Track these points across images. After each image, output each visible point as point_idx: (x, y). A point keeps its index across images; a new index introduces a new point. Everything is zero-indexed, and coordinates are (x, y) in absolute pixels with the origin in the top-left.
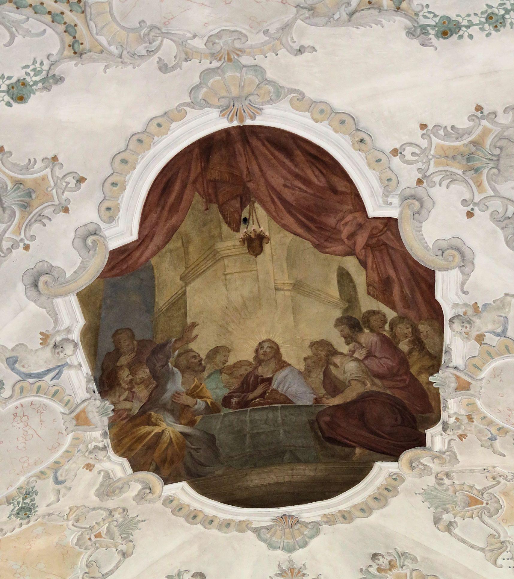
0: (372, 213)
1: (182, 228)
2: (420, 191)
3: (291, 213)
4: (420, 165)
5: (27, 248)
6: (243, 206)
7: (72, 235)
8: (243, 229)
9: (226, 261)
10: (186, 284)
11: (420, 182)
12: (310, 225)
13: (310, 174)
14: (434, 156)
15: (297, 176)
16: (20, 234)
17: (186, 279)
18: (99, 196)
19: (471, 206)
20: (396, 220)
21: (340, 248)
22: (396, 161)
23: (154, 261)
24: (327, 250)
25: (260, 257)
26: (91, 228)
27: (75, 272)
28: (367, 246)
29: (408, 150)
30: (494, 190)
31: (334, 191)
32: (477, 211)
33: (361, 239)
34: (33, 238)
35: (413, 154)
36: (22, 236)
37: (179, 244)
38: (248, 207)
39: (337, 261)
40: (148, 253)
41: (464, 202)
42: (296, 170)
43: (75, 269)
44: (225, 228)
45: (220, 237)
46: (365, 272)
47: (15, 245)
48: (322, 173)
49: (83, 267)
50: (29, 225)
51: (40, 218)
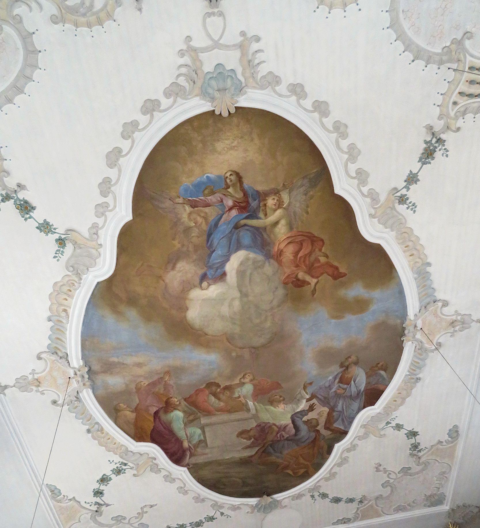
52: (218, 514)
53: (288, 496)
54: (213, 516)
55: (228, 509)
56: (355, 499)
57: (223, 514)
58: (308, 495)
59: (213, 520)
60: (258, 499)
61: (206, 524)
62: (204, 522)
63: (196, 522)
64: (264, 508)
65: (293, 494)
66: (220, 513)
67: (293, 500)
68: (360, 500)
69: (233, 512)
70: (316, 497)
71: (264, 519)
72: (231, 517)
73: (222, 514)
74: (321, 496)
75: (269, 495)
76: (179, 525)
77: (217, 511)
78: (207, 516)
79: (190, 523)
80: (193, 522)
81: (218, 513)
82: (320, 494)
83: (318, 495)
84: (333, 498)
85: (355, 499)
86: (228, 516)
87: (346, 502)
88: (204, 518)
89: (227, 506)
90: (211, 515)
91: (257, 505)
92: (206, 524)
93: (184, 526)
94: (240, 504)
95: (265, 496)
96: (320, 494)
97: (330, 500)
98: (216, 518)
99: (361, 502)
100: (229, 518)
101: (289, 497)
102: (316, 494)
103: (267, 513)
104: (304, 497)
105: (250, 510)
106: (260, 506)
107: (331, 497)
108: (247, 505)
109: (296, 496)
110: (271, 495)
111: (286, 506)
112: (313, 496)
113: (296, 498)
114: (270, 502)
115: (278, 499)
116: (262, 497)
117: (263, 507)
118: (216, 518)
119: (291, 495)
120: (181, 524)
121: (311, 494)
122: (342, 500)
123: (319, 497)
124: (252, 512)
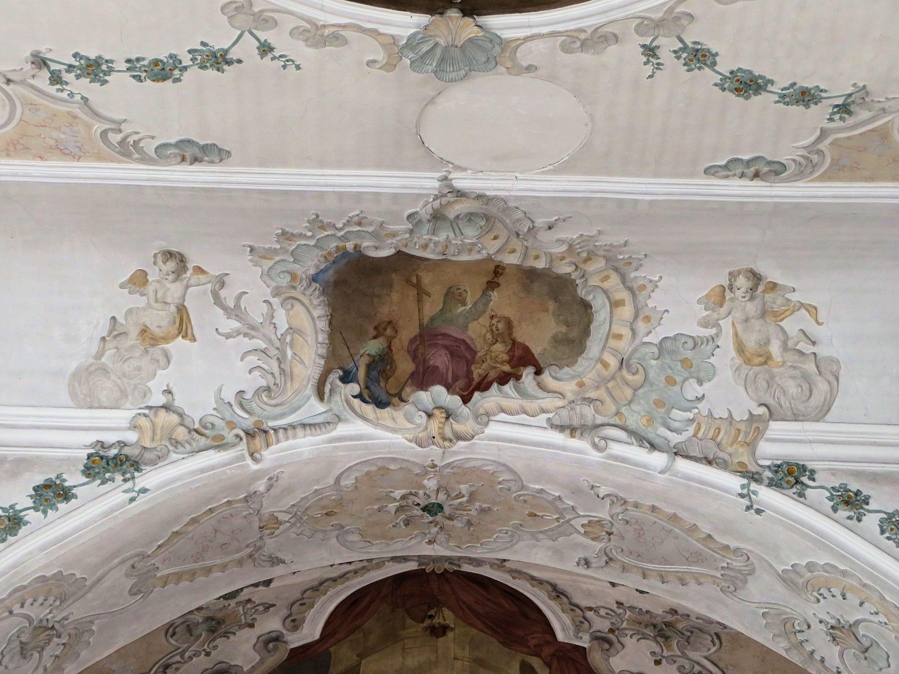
0: (561, 636)
1: (366, 626)
2: (611, 636)
3: (479, 619)
4: (614, 621)
5: (208, 654)
6: (430, 608)
7: (254, 641)
8: (427, 622)
9: (406, 641)
10: (362, 659)
11: (611, 631)
12: (499, 630)
13: (503, 602)
14: (627, 620)
15: (488, 600)
16: (203, 646)
17: (361, 656)
18: (285, 612)
19: (660, 657)
20: (585, 648)
21: (525, 650)
22: (590, 614)
23: (332, 649)
24: (512, 648)
25: (441, 639)
26: (273, 635)
27: (253, 667)
28: (553, 655)
29: (603, 612)
30: (683, 653)
31: (526, 616)
32: (664, 661)
33: (547, 651)
34: (215, 647)
35: (607, 614)
36: (206, 647)
37: (361, 635)
38: (435, 609)
39: (520, 657)
40: (328, 645)
41: (653, 653)
42: (490, 597)
43: (253, 664)
44: (409, 621)
45: (404, 627)
46: (548, 670)
47: (196, 654)
48: (515, 604)
49: (262, 661)
50: (214, 640)
51: (226, 635)
52: (247, 49)
53: (545, 30)
54: (226, 51)
55: (291, 33)
56: (823, 95)
57: (271, 49)
58: (632, 47)
59: (226, 67)
60: (421, 19)
61: (193, 75)
62: (185, 68)
63: (156, 62)
64: (442, 60)
65: (572, 26)
66: (257, 44)
67: (566, 48)
68: (840, 101)
69: (310, 51)
70: (665, 55)
71: (432, 101)
72: (298, 67)
73: (265, 49)
74: (684, 55)
75: (470, 10)
76: (81, 58)
77: (247, 34)
78: (203, 44)
79: (129, 61)
80: (144, 59)
81: (249, 45)
82: (685, 48)
83: (675, 52)
84: (732, 72)
85: (823, 95)
86: (287, 61)
87: (783, 98)
88: (190, 52)
89: (289, 23)
90: (219, 44)
91: (412, 43)
92: (193, 75)
93: (104, 67)
94: (344, 26)
95: (454, 14)
96: (685, 48)
97: (717, 78)
98: (239, 61)
99: (844, 109)
100: (291, 68)
101: (553, 34)
102: (667, 45)
103: (451, 81)
104: (613, 49)
105: (380, 56)
106: (425, 48)
107: (724, 66)
108: (374, 33)
109: (583, 36)
110: (479, 15)
111: (530, 69)
112: (650, 51)
113: (578, 44)
114: (471, 40)
115: (507, 35)
116: (441, 14)
117: (438, 52)
118: (239, 61)
119: (560, 28)
120: (93, 56)
121: (647, 41)
122: (770, 88)
123: (678, 58)
124: (389, 66)
